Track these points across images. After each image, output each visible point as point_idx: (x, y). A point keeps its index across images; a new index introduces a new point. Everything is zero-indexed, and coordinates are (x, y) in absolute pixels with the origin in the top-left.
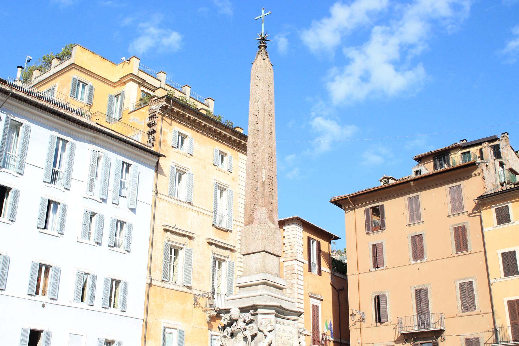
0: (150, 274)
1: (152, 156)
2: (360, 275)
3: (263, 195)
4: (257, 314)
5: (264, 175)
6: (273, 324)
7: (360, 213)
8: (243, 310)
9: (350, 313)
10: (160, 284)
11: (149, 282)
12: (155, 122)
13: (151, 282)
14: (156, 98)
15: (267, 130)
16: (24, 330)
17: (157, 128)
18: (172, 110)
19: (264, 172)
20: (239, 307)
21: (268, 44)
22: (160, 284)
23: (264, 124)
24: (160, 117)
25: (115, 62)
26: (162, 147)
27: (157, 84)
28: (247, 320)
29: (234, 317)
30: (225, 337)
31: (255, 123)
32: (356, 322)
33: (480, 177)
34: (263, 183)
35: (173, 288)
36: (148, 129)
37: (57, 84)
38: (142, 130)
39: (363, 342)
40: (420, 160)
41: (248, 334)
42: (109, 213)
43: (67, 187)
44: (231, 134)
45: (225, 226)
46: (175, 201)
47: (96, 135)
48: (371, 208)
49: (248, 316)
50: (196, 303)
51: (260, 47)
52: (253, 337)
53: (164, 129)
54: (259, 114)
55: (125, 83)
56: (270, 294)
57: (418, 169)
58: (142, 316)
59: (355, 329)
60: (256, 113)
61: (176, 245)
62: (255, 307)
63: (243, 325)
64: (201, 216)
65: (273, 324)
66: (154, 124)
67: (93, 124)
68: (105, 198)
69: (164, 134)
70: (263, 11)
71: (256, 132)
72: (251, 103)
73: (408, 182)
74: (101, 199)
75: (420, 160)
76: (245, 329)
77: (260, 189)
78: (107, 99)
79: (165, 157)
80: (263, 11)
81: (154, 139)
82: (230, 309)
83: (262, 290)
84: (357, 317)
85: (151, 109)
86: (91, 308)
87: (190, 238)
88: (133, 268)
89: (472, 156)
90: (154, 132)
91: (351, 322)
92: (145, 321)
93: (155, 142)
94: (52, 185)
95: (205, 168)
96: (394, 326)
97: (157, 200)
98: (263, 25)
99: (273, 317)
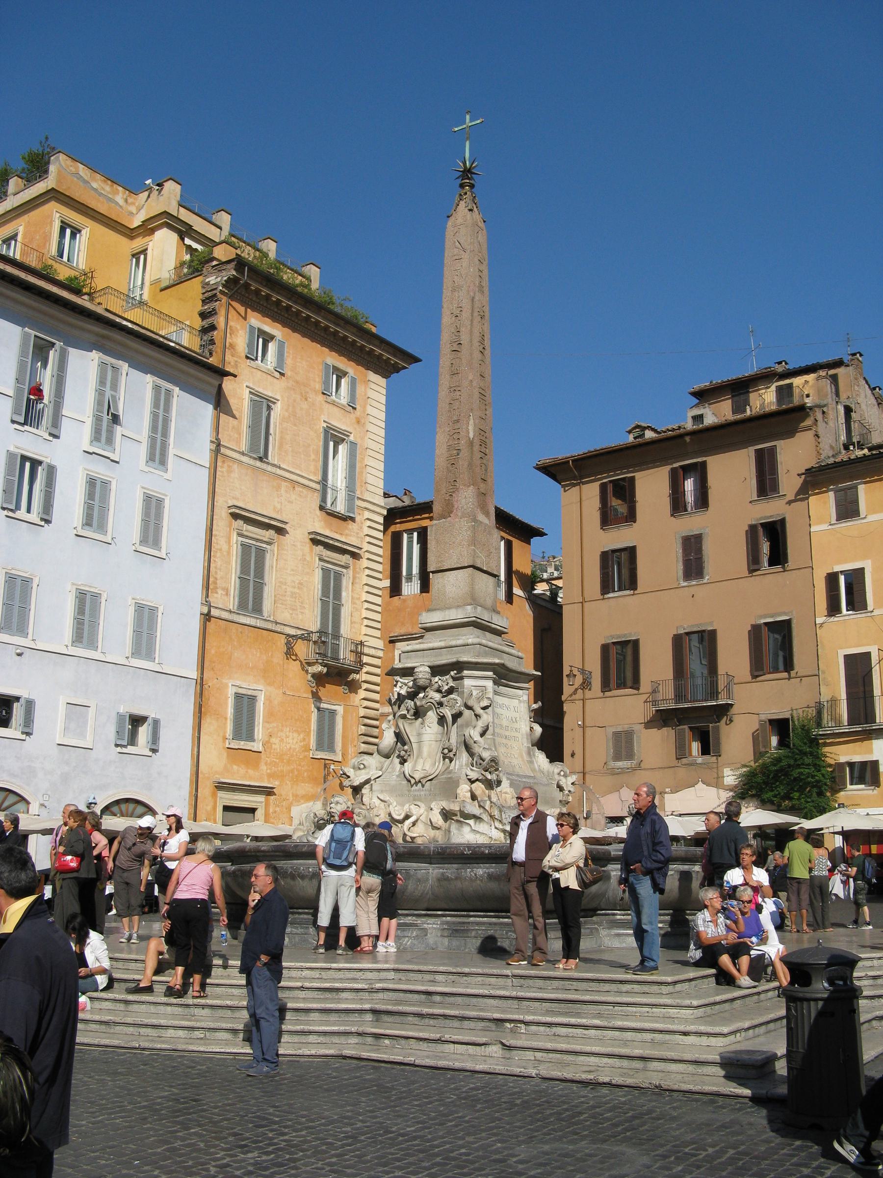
0: (207, 596)
1: (201, 372)
2: (586, 605)
3: (470, 465)
4: (462, 678)
5: (471, 428)
6: (490, 695)
7: (591, 492)
8: (437, 670)
9: (566, 671)
11: (205, 611)
12: (214, 310)
13: (209, 611)
14: (215, 263)
15: (476, 344)
17: (220, 320)
19: (471, 422)
20: (429, 664)
21: (477, 180)
23: (471, 332)
24: (224, 299)
25: (134, 188)
26: (228, 357)
27: (213, 233)
28: (446, 688)
29: (421, 682)
30: (404, 717)
31: (453, 330)
32: (576, 690)
33: (810, 434)
34: (471, 443)
35: (248, 623)
36: (198, 323)
37: (21, 229)
38: (188, 323)
39: (587, 724)
40: (703, 396)
41: (448, 713)
43: (55, 432)
44: (356, 336)
45: (341, 508)
47: (105, 332)
48: (610, 481)
49: (445, 682)
50: (290, 652)
51: (462, 186)
52: (456, 716)
53: (231, 323)
54: (463, 313)
55: (152, 231)
56: (484, 642)
57: (697, 412)
58: (194, 674)
59: (573, 701)
60: (457, 312)
62: (459, 666)
63: (437, 696)
64: (299, 489)
65: (490, 695)
66: (213, 313)
67: (100, 310)
70: (468, 117)
71: (455, 347)
72: (446, 293)
73: (681, 436)
75: (703, 396)
76: (441, 704)
77: (465, 453)
79: (235, 376)
80: (468, 117)
81: (212, 342)
82: (413, 668)
83: (471, 636)
84: (579, 680)
85: (208, 284)
87: (281, 531)
89: (796, 391)
90: (213, 328)
91: (567, 690)
92: (199, 681)
94: (26, 428)
95: (306, 399)
96: (645, 697)
98: (468, 143)
99: (489, 684)
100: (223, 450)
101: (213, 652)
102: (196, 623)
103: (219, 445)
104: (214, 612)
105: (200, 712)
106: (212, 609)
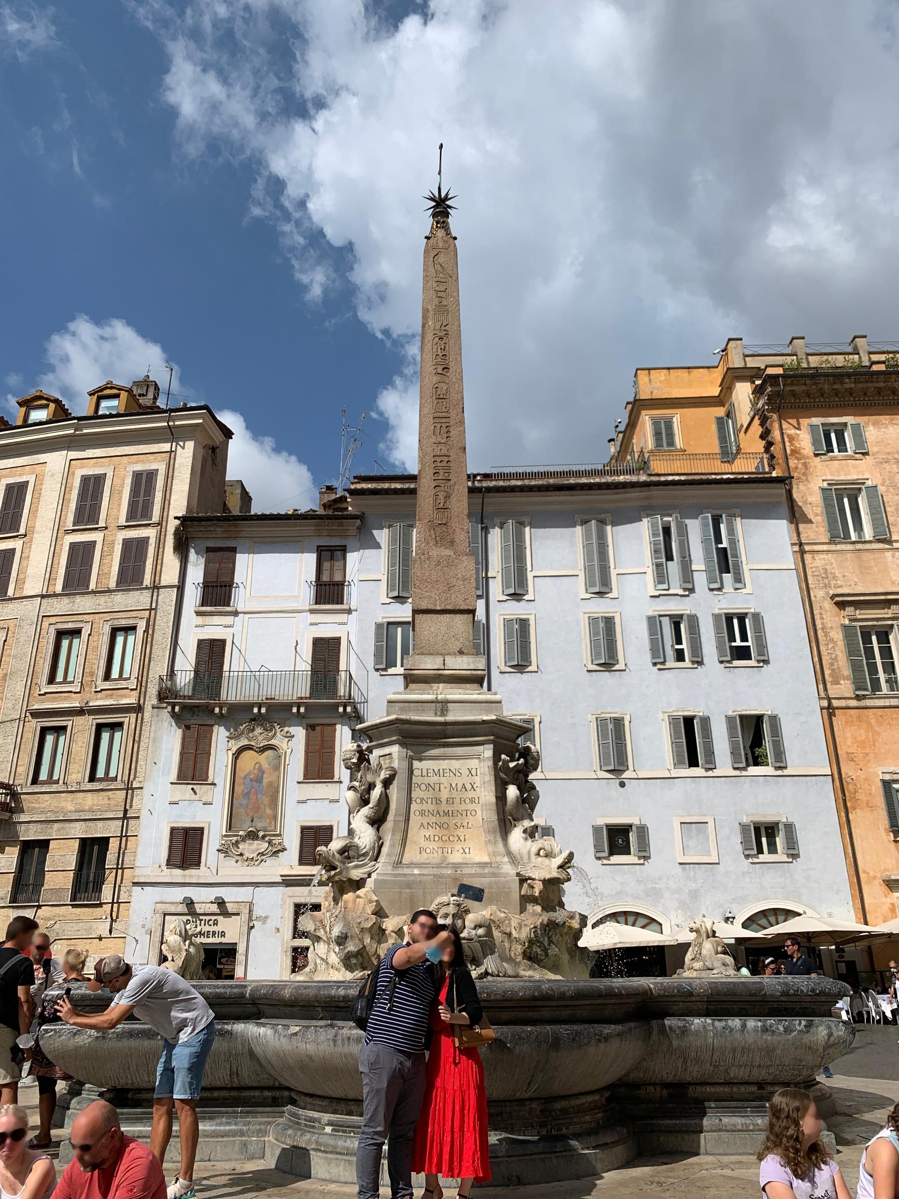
0: (826, 689)
10: (854, 703)
11: (825, 703)
13: (830, 703)
16: (597, 830)
17: (776, 434)
18: (793, 394)
22: (854, 703)
24: (775, 416)
26: (792, 463)
42: (706, 605)
46: (850, 547)
61: (875, 623)
65: (396, 765)
68: (690, 586)
69: (792, 439)
74: (685, 589)
78: (714, 427)
81: (772, 457)
86: (710, 773)
88: (783, 687)
93: (774, 462)
97: (808, 557)
100: (807, 548)
101: (849, 742)
102: (817, 720)
103: (801, 545)
104: (835, 703)
105: (845, 807)
106: (833, 701)
